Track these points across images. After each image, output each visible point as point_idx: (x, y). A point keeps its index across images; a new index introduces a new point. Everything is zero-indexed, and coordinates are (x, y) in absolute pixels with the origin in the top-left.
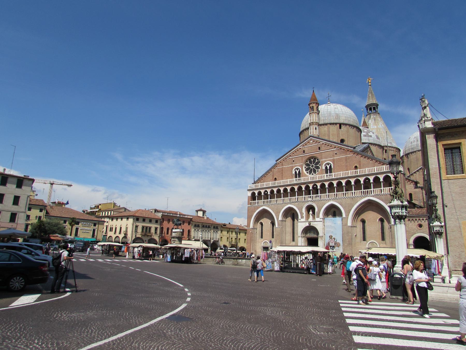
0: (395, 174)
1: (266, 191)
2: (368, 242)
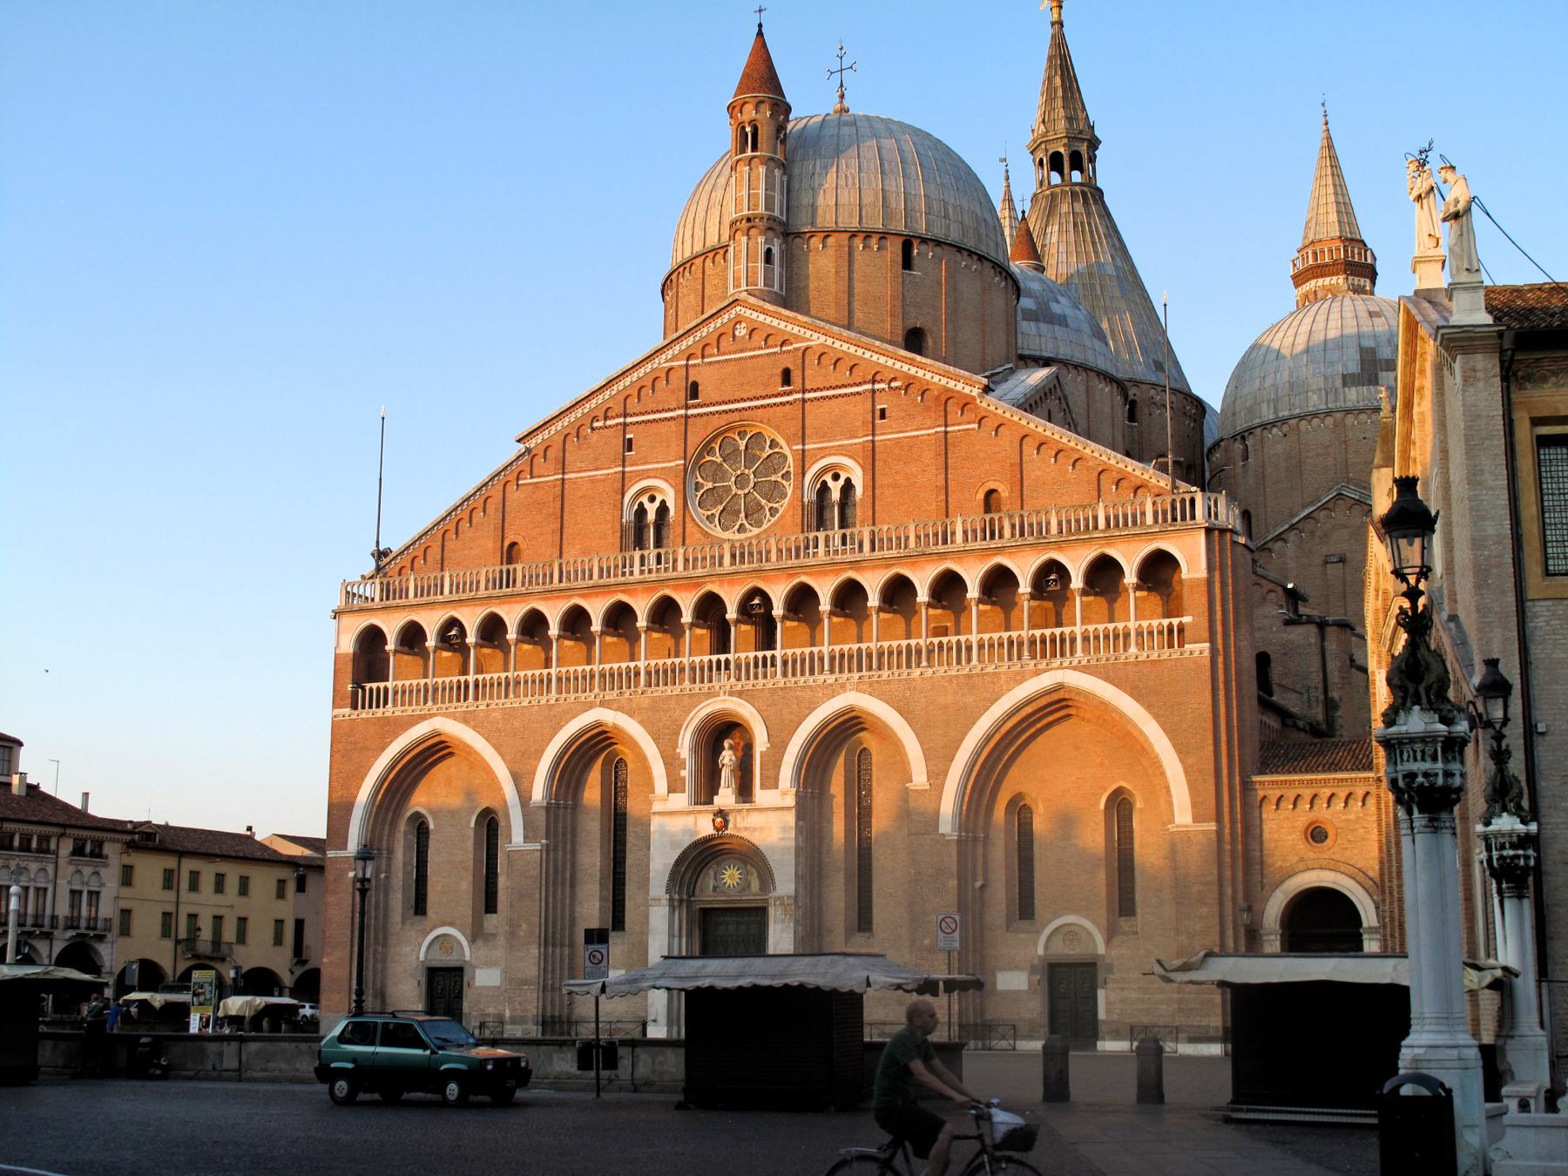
0: (1412, 580)
1: (453, 622)
2: (1045, 926)
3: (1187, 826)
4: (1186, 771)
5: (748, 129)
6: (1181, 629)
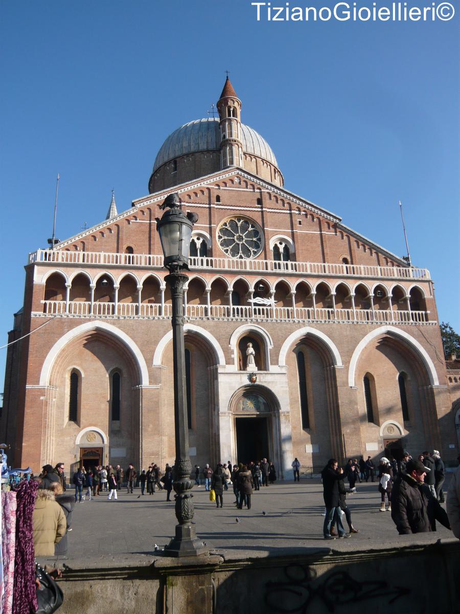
4: (435, 366)
5: (232, 109)
6: (426, 314)
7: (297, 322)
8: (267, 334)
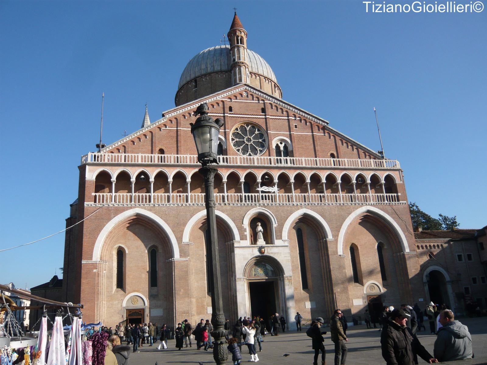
3: (409, 253)
4: (406, 237)
5: (239, 38)
6: (398, 196)
7: (296, 205)
8: (273, 216)
